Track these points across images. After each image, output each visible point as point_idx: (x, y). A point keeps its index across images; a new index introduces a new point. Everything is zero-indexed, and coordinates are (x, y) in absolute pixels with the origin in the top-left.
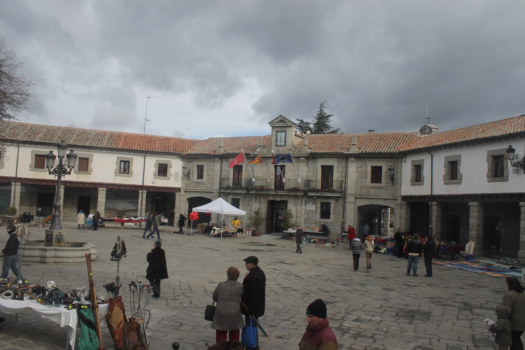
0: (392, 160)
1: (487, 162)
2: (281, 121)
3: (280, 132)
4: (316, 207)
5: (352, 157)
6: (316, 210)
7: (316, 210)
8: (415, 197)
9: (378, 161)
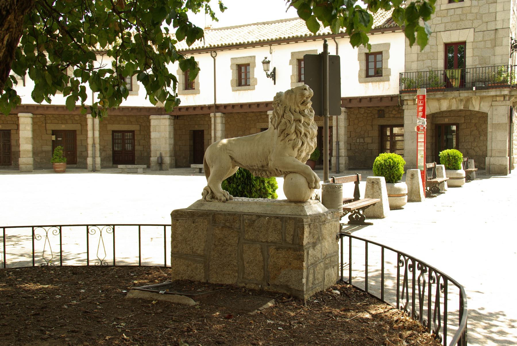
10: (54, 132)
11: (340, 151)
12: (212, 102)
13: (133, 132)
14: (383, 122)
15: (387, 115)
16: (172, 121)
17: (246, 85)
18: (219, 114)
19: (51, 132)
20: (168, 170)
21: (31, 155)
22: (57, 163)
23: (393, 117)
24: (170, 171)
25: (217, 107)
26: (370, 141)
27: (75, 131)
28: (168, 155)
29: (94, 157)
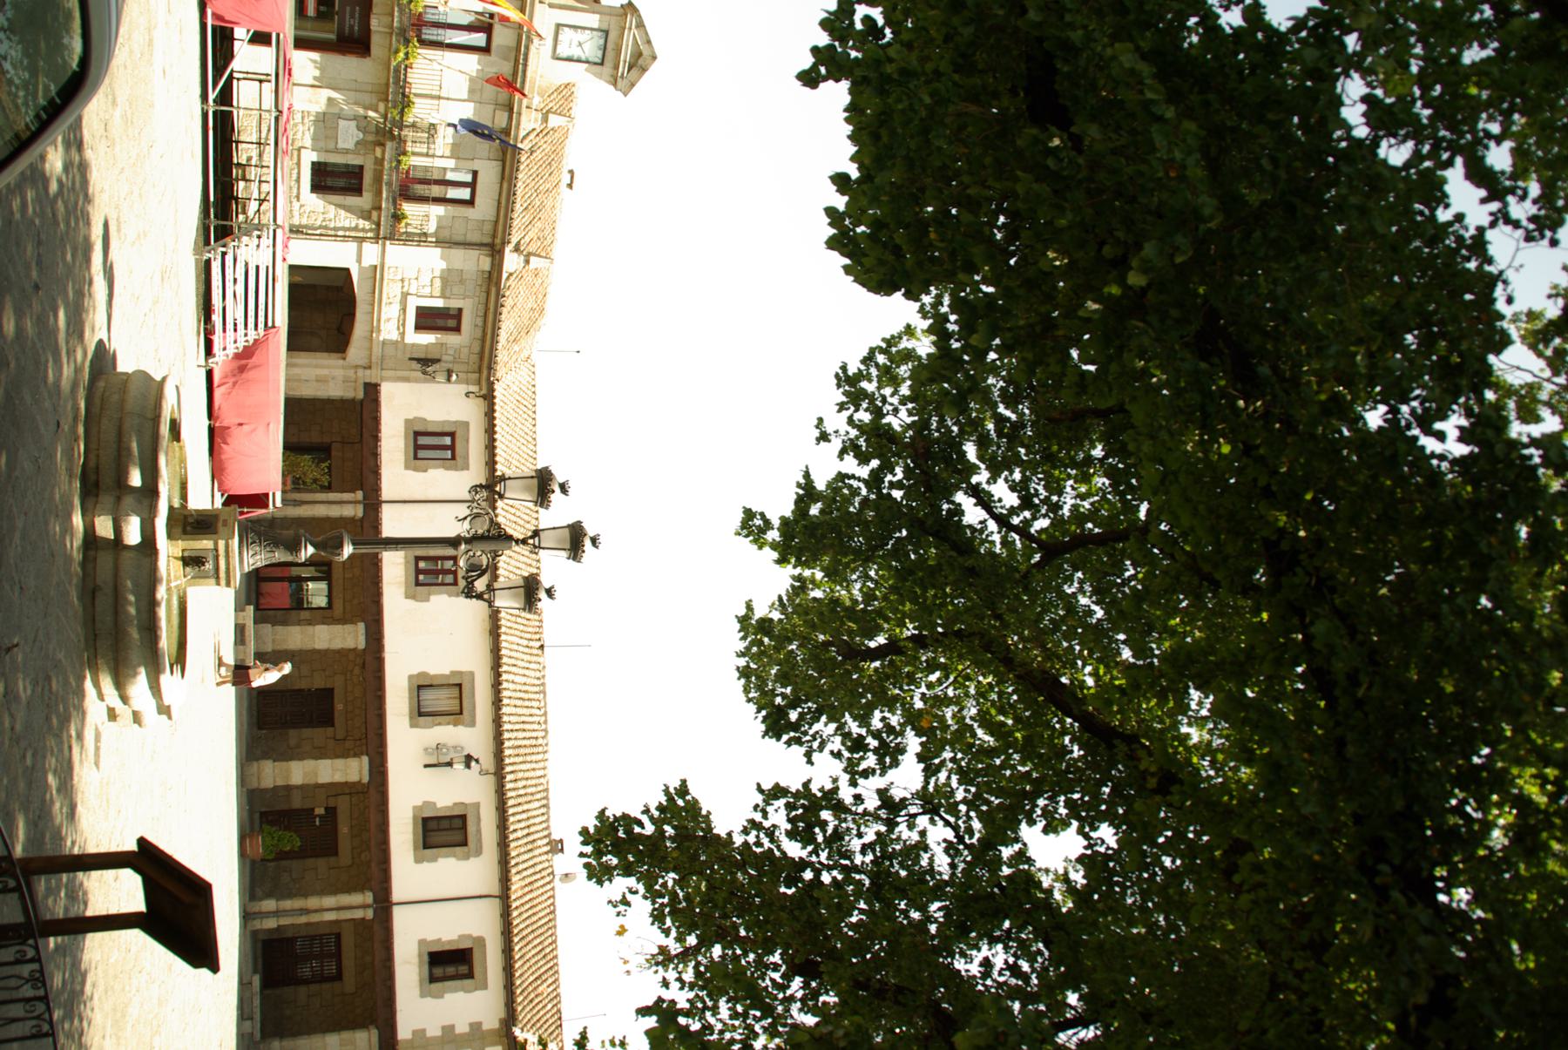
0: (475, 358)
1: (452, 672)
2: (638, 55)
3: (602, 42)
4: (347, 151)
5: (493, 265)
6: (337, 151)
7: (337, 151)
8: (376, 438)
9: (476, 326)
10: (331, 812)
13: (339, 976)
19: (331, 804)
21: (280, 783)
22: (263, 841)
27: (336, 854)
29: (277, 913)
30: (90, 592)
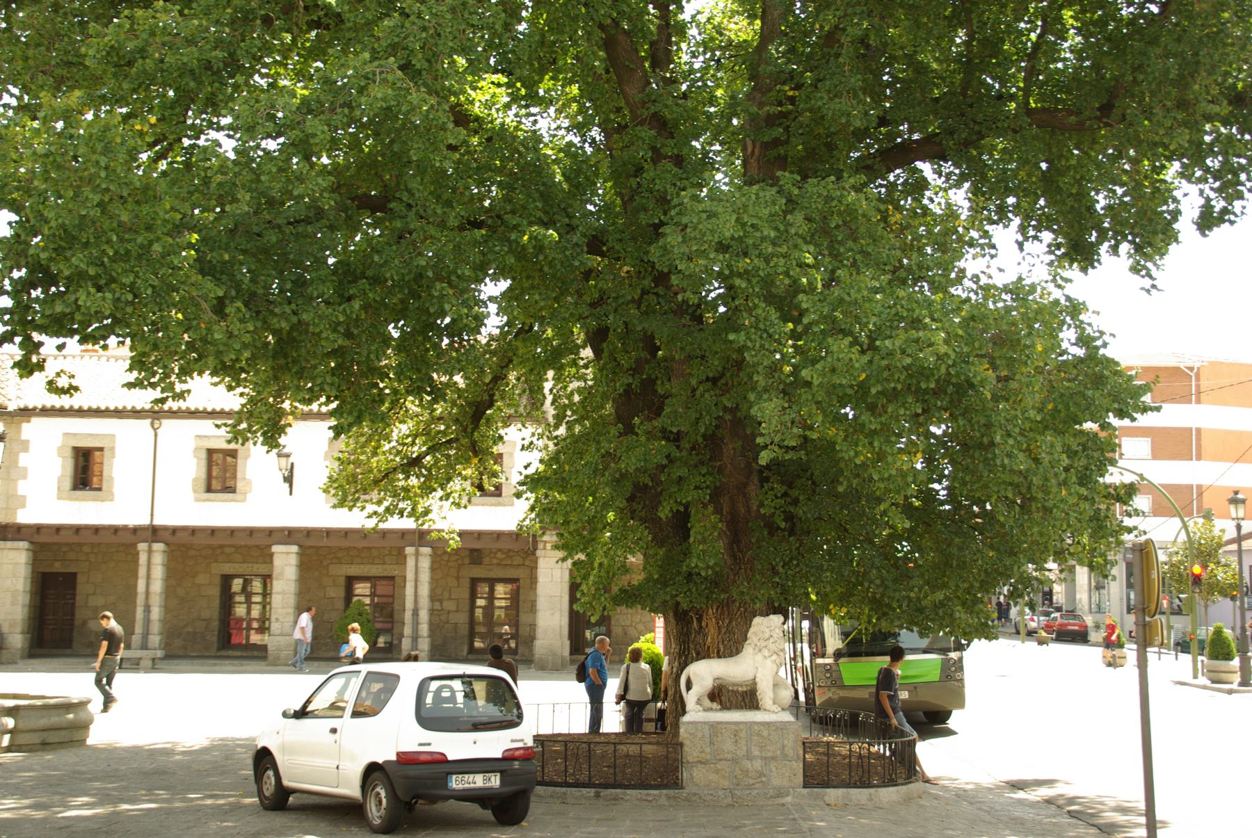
11: (420, 627)
12: (144, 520)
14: (478, 572)
15: (486, 560)
16: (31, 554)
17: (231, 490)
18: (159, 547)
20: (15, 663)
23: (498, 564)
24: (21, 664)
25: (154, 533)
26: (454, 608)
28: (19, 629)
30: (45, 746)
